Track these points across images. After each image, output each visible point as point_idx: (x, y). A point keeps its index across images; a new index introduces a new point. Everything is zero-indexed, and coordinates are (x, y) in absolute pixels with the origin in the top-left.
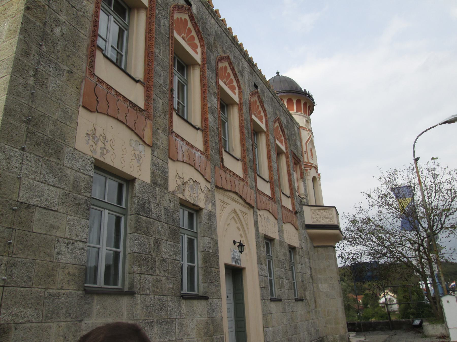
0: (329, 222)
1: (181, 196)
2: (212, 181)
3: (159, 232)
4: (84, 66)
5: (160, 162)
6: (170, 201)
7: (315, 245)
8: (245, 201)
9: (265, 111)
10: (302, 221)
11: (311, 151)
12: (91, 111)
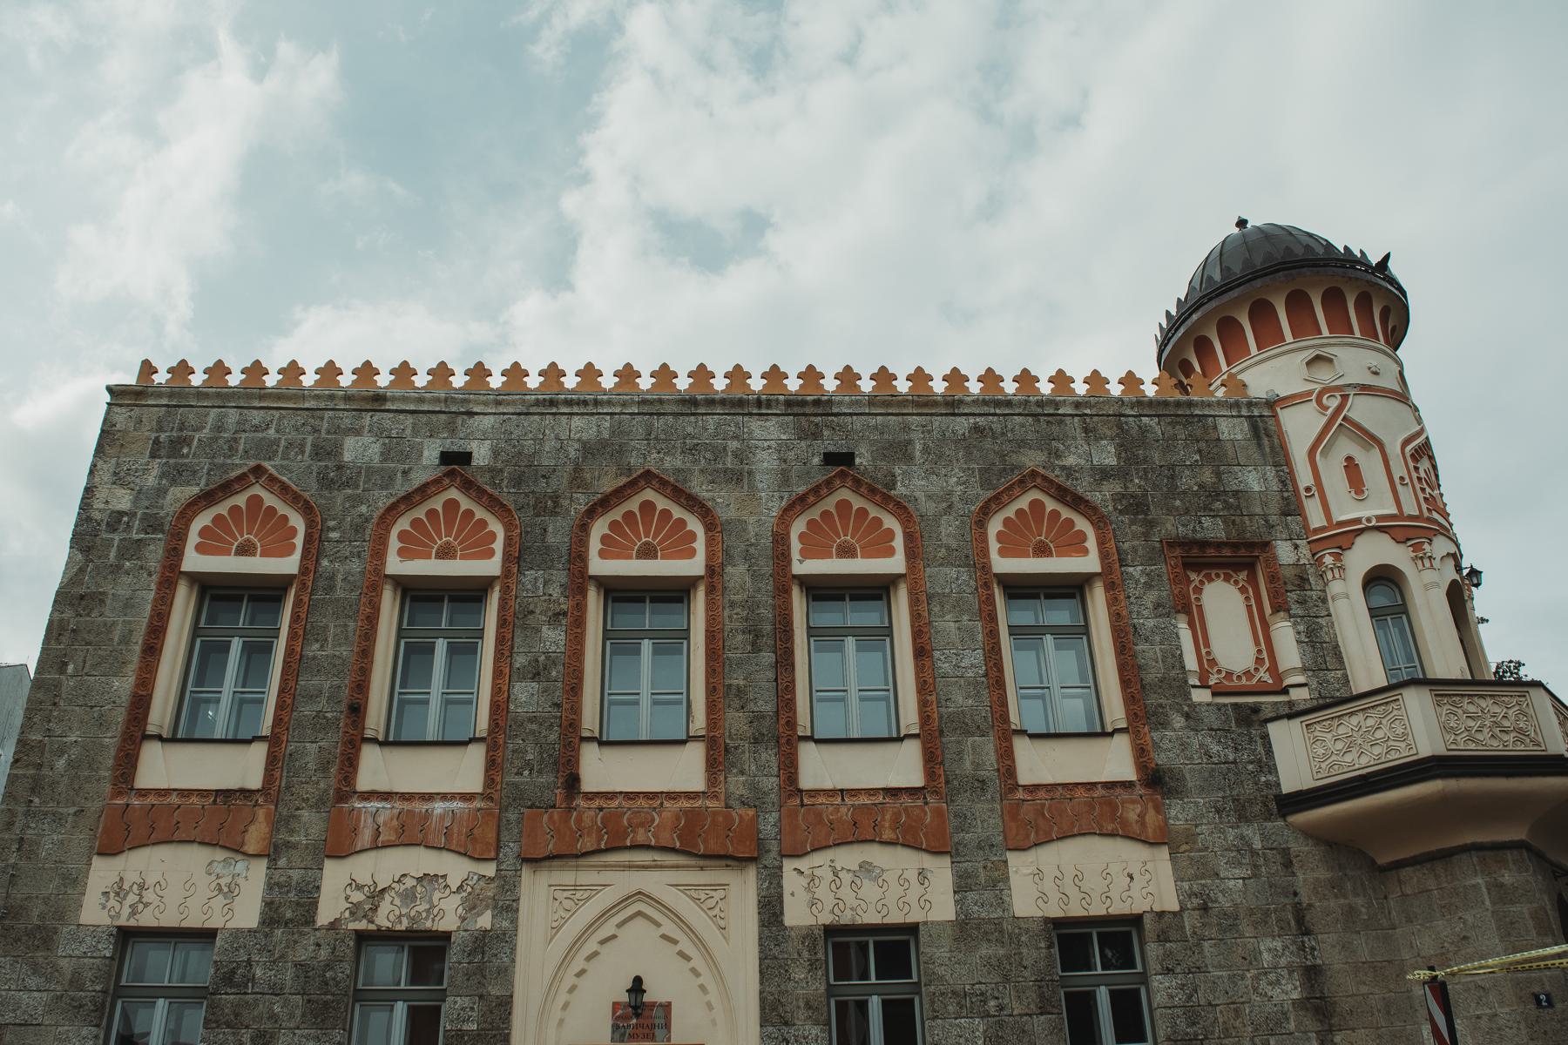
0: (1393, 755)
1: (362, 925)
2: (511, 850)
3: (273, 1017)
4: (107, 788)
5: (296, 875)
6: (318, 945)
7: (1382, 860)
8: (696, 855)
9: (900, 509)
10: (1248, 789)
11: (1351, 466)
12: (115, 854)
